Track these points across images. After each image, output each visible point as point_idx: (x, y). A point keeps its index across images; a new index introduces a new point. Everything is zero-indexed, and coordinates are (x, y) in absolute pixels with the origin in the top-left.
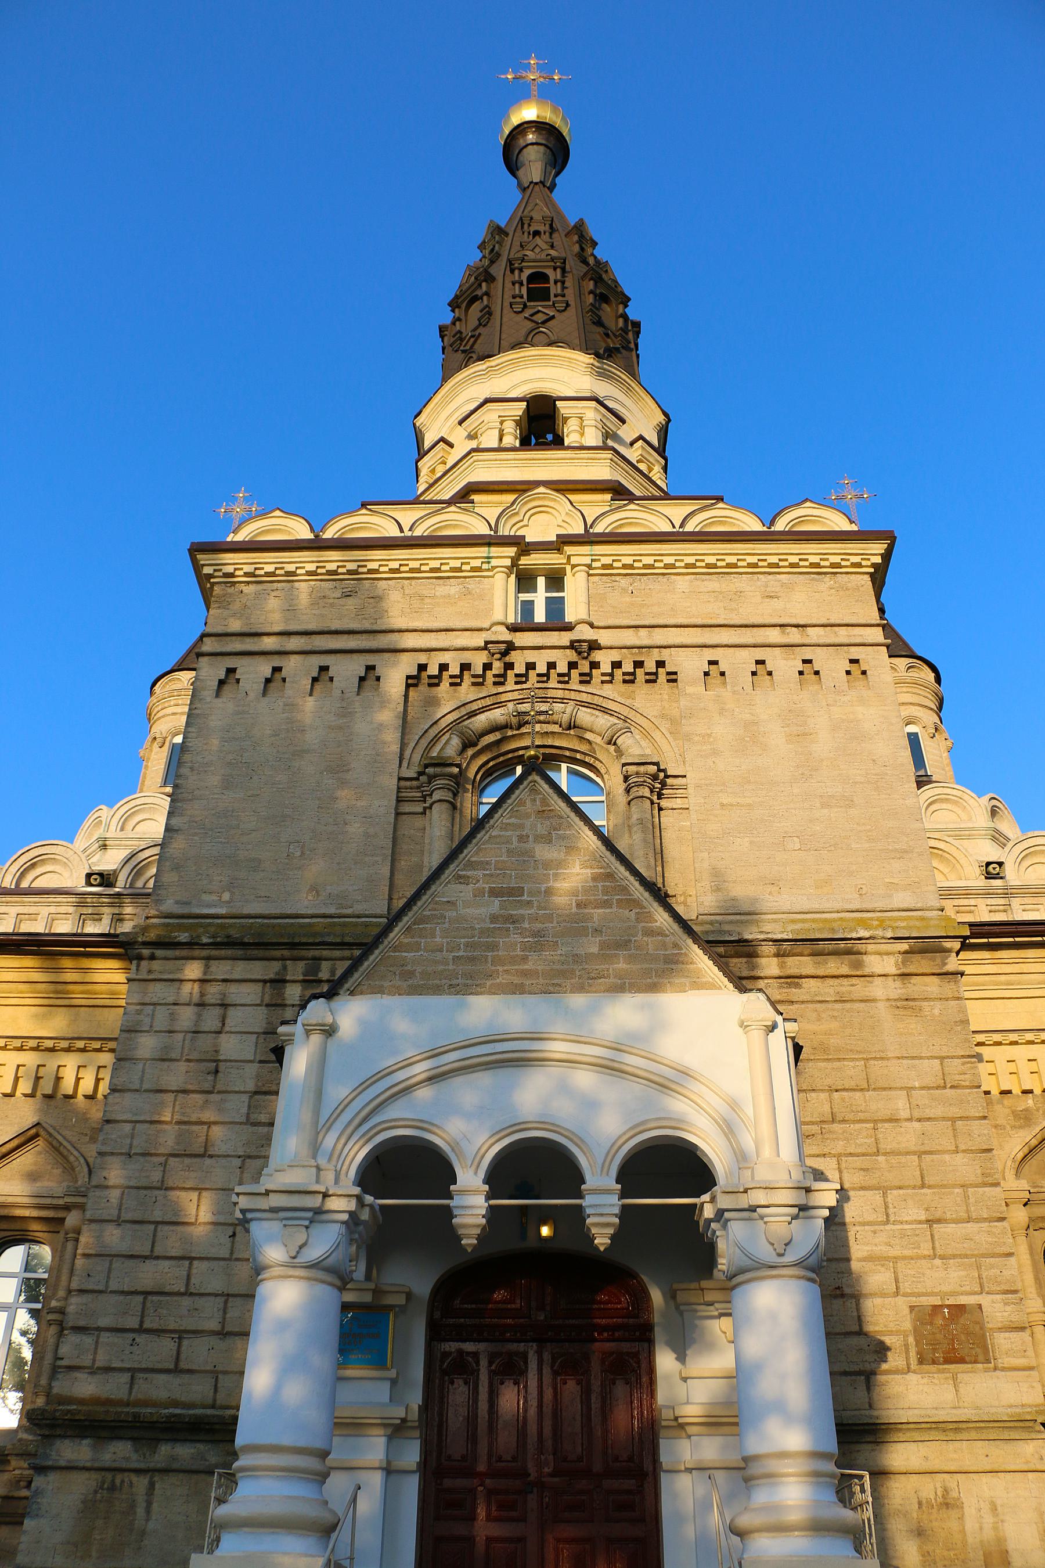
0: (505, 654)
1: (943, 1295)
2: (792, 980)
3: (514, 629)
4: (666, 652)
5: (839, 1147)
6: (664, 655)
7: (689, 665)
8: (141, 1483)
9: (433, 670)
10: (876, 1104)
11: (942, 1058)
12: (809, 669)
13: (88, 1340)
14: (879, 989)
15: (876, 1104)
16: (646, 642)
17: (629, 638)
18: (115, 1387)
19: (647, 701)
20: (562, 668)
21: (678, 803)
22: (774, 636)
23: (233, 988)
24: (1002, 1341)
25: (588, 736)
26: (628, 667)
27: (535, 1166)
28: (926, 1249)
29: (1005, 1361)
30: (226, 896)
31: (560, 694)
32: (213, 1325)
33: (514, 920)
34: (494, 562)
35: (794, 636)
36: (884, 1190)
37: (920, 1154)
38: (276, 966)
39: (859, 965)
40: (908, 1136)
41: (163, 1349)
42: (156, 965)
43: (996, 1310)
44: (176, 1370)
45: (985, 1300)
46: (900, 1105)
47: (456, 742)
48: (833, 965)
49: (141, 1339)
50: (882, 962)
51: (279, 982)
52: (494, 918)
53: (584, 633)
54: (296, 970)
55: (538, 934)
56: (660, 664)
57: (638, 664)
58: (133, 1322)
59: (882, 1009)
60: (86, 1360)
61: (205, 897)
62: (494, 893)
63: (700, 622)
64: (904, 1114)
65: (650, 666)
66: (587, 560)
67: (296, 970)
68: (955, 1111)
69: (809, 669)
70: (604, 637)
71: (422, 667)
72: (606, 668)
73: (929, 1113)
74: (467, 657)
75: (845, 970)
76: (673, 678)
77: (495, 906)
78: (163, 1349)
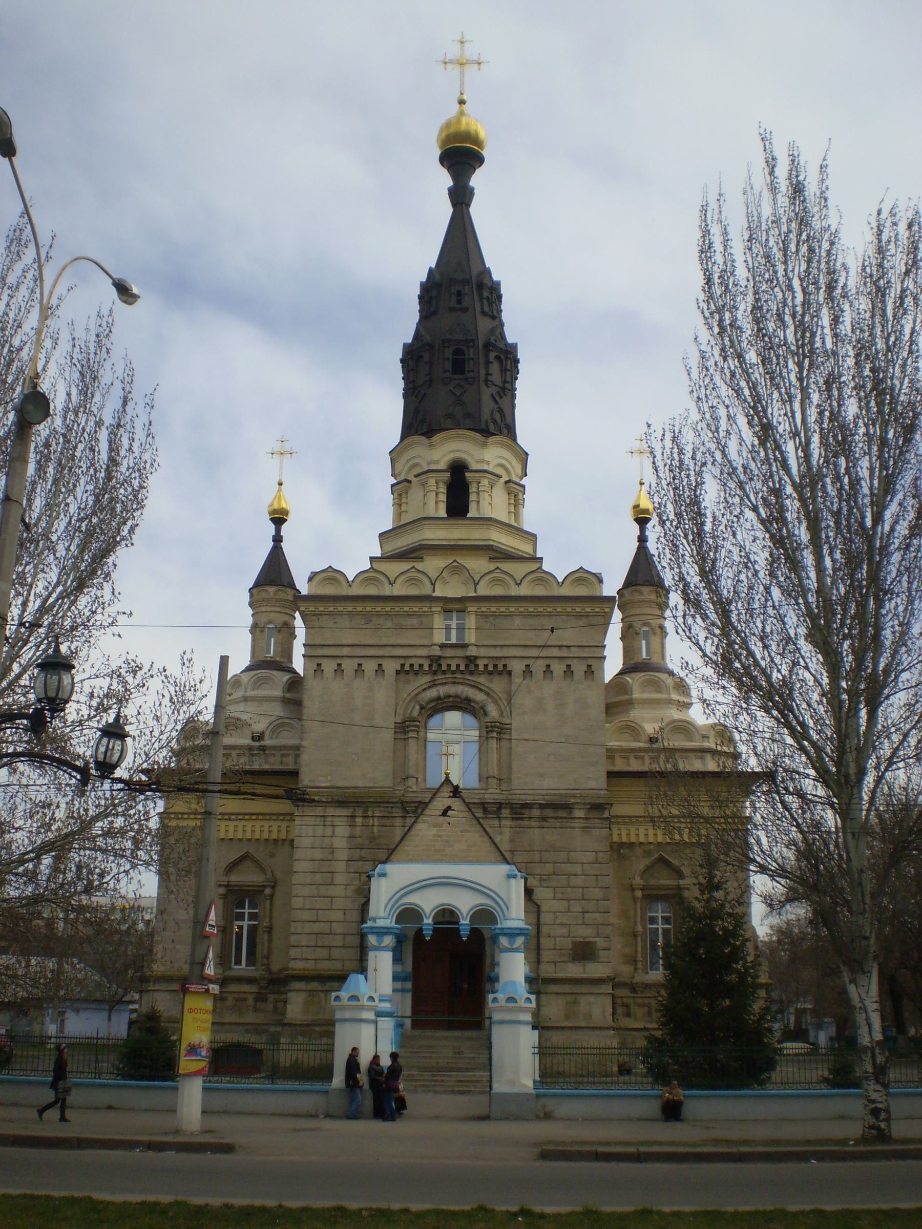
0: (437, 660)
1: (584, 938)
2: (544, 819)
3: (442, 646)
4: (507, 660)
5: (554, 884)
6: (507, 662)
7: (517, 667)
8: (322, 995)
9: (407, 668)
10: (570, 868)
11: (596, 852)
12: (569, 672)
13: (298, 950)
14: (577, 824)
15: (570, 868)
16: (500, 655)
17: (494, 653)
18: (310, 965)
19: (497, 685)
20: (462, 668)
21: (507, 736)
22: (556, 652)
23: (336, 819)
24: (602, 953)
25: (472, 704)
26: (490, 668)
27: (447, 915)
28: (580, 922)
29: (601, 960)
30: (329, 778)
31: (461, 681)
32: (340, 944)
33: (440, 836)
34: (433, 609)
35: (564, 653)
36: (568, 900)
37: (583, 888)
38: (351, 810)
39: (570, 813)
40: (578, 881)
41: (323, 953)
42: (305, 809)
43: (600, 943)
44: (329, 959)
45: (597, 939)
46: (578, 869)
47: (417, 707)
48: (562, 813)
49: (317, 949)
50: (579, 813)
51: (353, 817)
52: (434, 836)
53: (472, 651)
54: (359, 812)
55: (447, 841)
56: (505, 666)
57: (495, 666)
58: (313, 944)
59: (577, 832)
60: (299, 956)
61: (321, 779)
62: (434, 826)
63: (523, 643)
64: (580, 873)
65: (500, 668)
66: (475, 609)
67: (359, 812)
68: (598, 873)
69: (569, 672)
70: (482, 652)
71: (403, 665)
72: (481, 668)
73: (588, 873)
74: (421, 661)
75: (565, 815)
76: (510, 673)
77: (434, 831)
78: (323, 953)
